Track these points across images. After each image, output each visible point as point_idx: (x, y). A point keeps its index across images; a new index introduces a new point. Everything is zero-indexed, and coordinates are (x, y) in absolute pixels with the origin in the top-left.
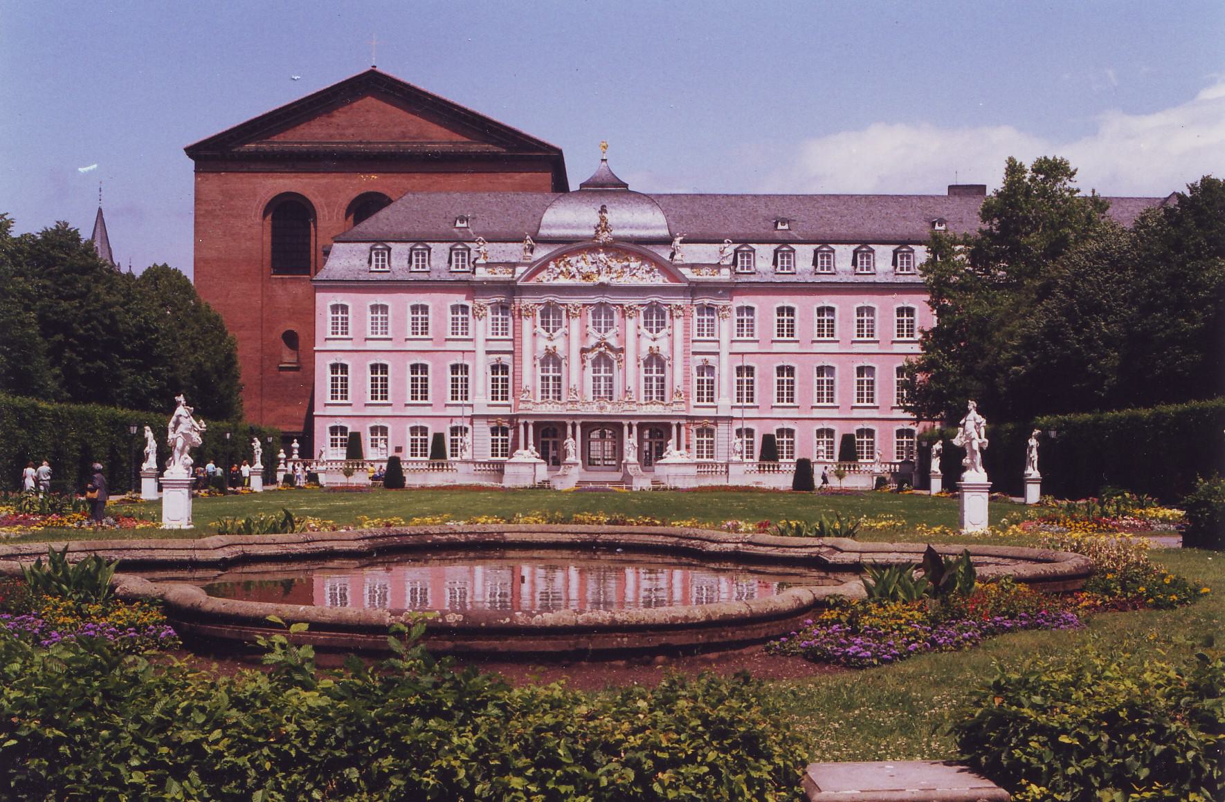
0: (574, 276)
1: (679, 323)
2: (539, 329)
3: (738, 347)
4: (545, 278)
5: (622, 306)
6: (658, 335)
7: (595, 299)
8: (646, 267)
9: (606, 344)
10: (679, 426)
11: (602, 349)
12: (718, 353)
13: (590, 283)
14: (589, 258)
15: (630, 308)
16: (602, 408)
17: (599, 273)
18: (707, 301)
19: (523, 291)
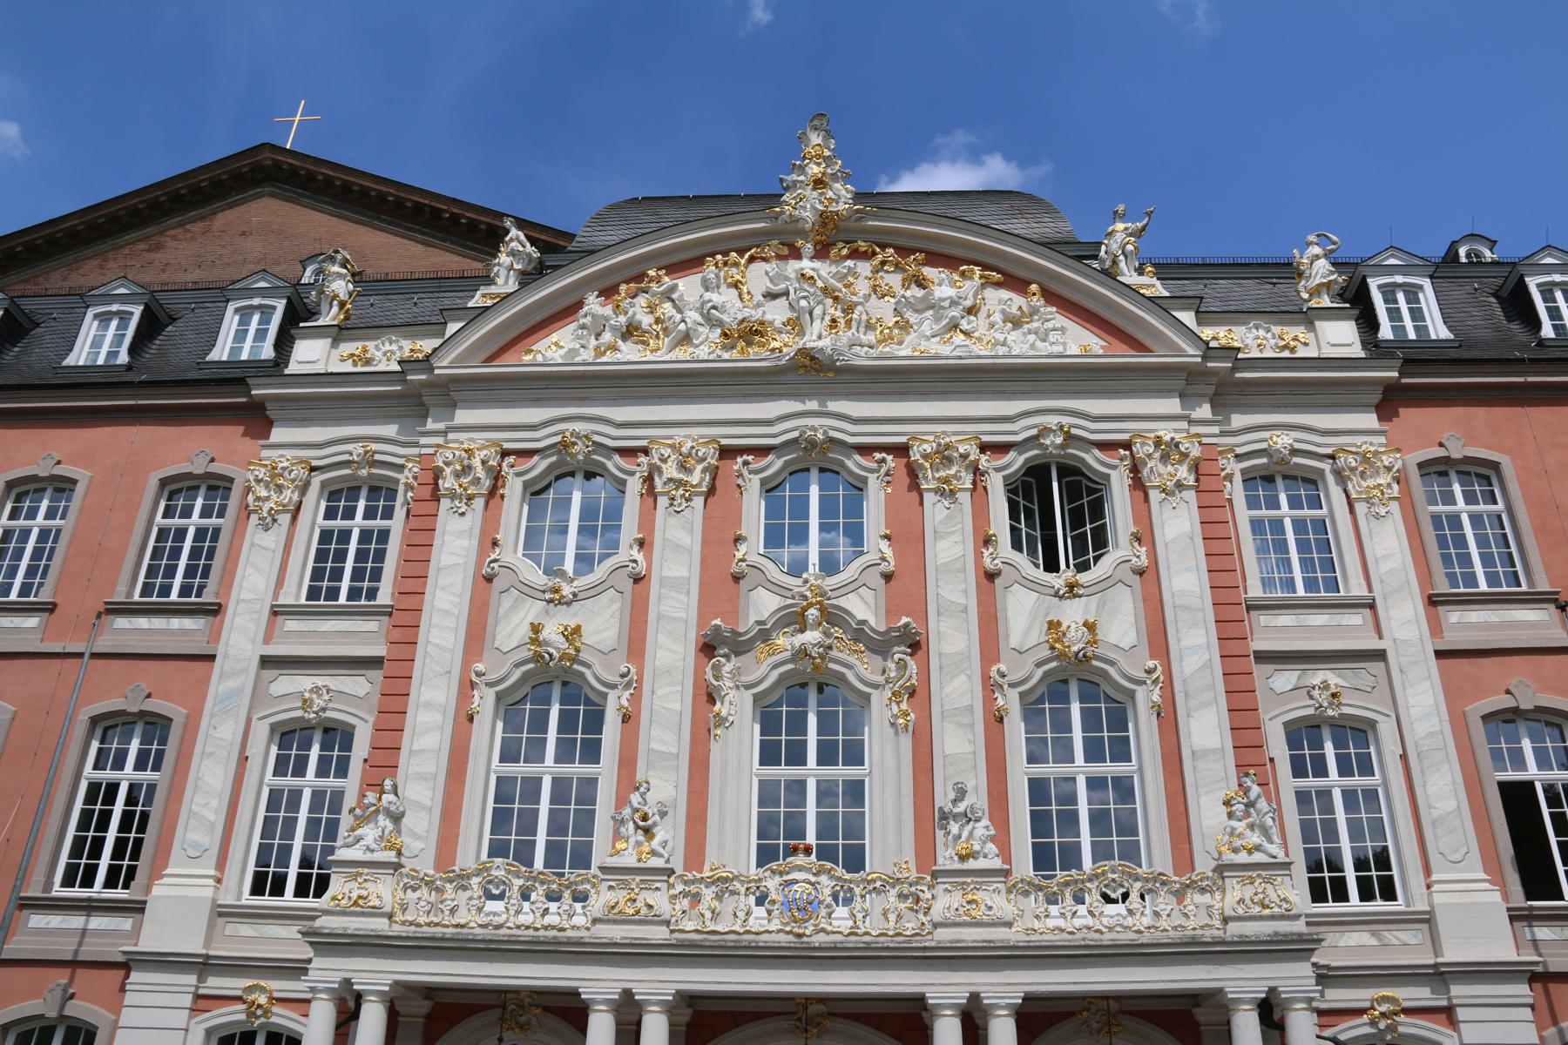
0: (686, 338)
1: (1178, 523)
2: (512, 553)
3: (1471, 625)
4: (557, 348)
5: (901, 450)
6: (1083, 578)
7: (777, 417)
8: (999, 300)
9: (833, 617)
10: (1271, 1013)
11: (812, 636)
12: (1380, 655)
13: (755, 357)
14: (758, 276)
15: (944, 455)
16: (803, 910)
17: (796, 325)
18: (1283, 441)
19: (452, 392)
